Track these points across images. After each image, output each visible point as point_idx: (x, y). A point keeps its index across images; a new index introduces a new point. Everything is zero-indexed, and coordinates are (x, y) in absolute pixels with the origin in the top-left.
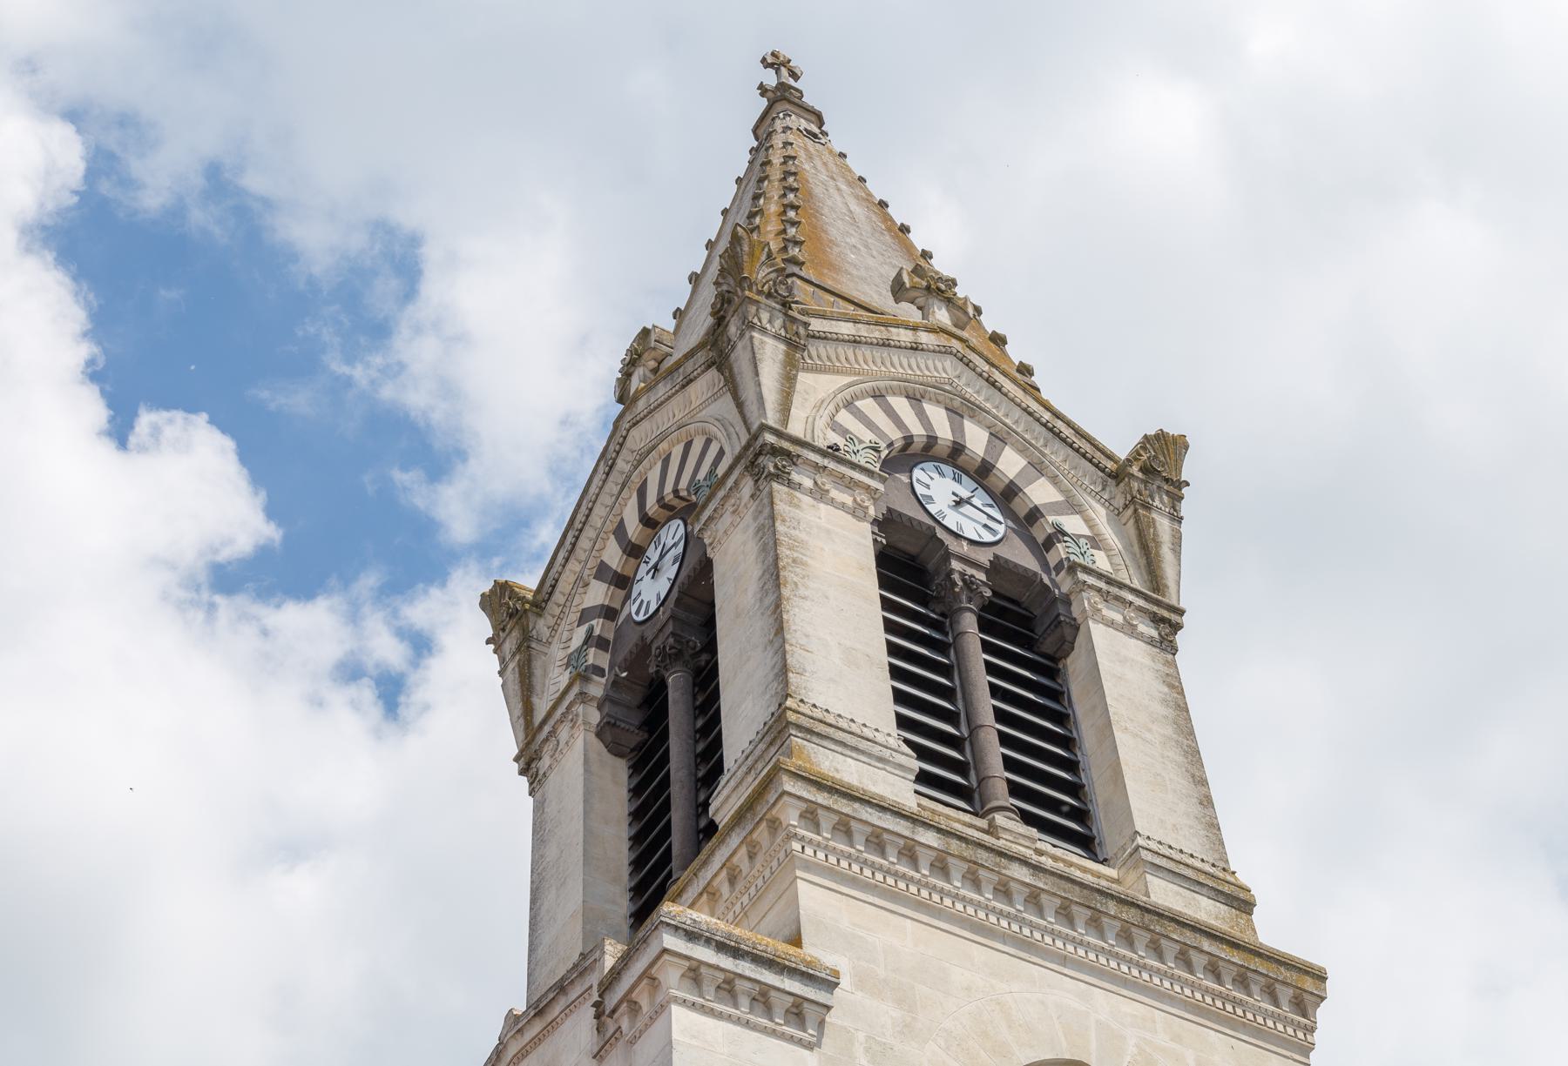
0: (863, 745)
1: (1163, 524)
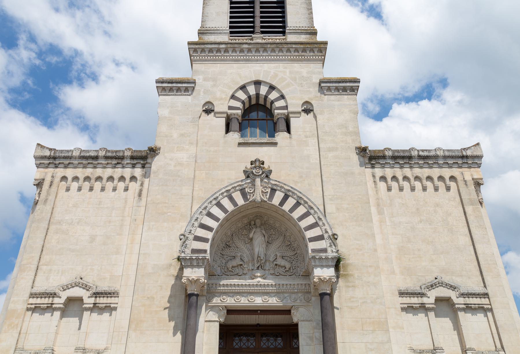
0: (216, 31)
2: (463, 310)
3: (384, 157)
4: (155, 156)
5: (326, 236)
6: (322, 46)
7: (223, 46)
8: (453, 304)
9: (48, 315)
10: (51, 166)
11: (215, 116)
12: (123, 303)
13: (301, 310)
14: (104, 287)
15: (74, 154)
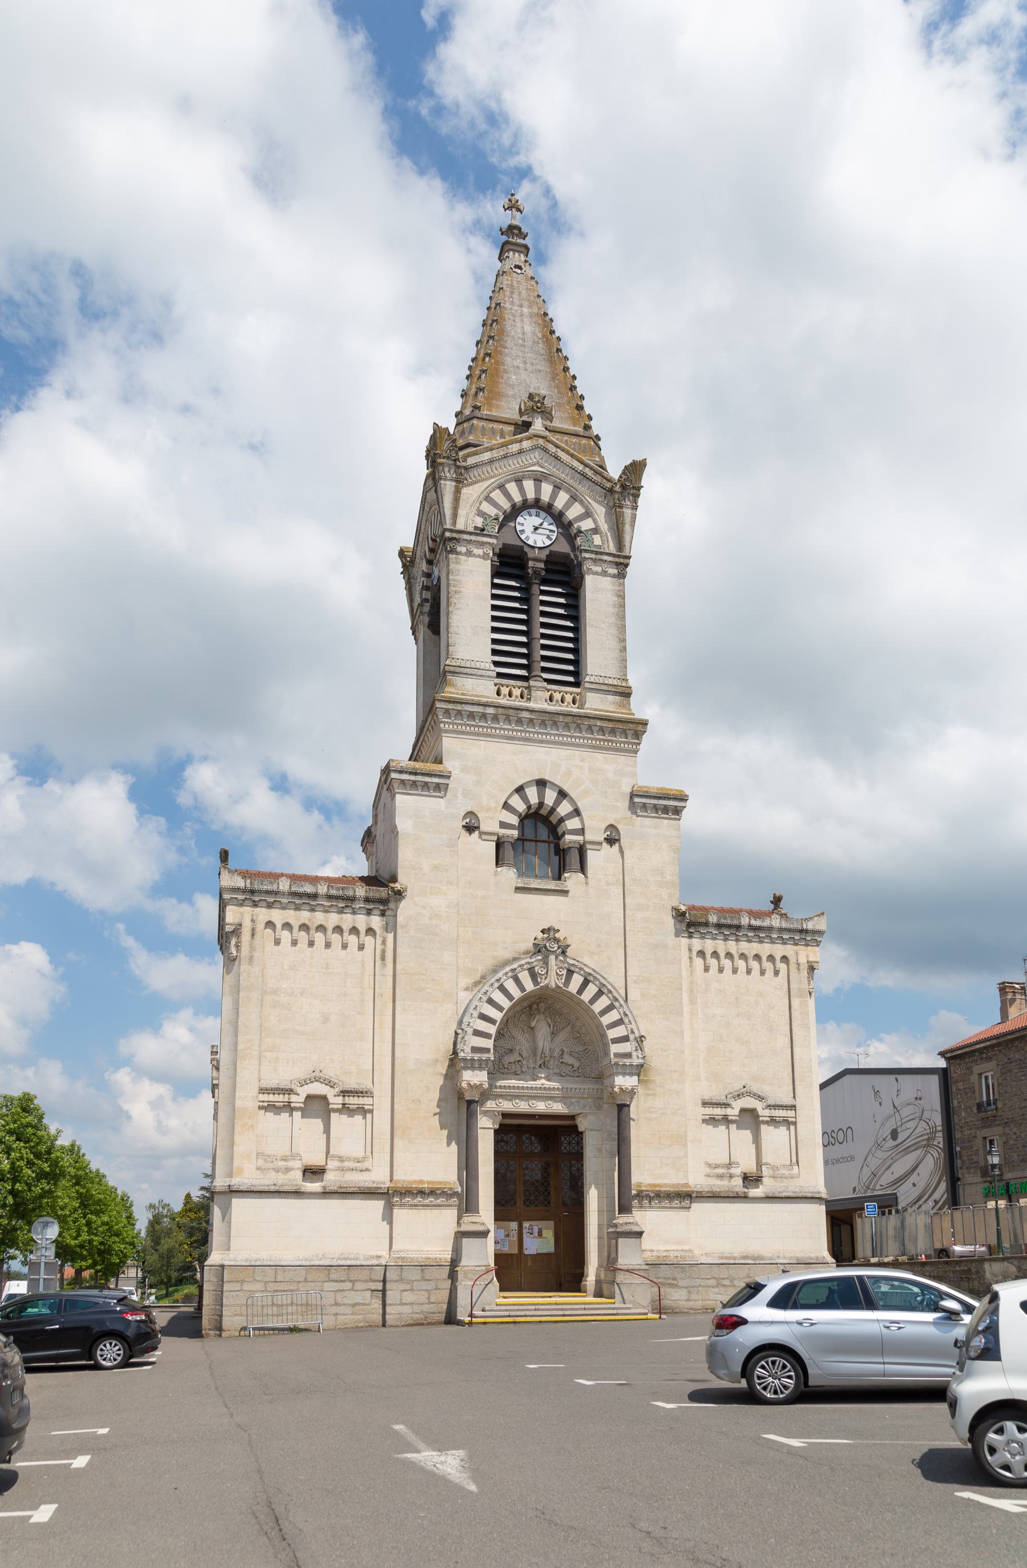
0: (475, 672)
1: (628, 512)
2: (767, 1123)
3: (706, 924)
4: (400, 900)
5: (632, 1037)
6: (640, 728)
7: (490, 711)
8: (758, 1116)
9: (285, 1116)
10: (247, 902)
11: (480, 837)
12: (381, 1103)
13: (590, 1118)
14: (352, 1084)
15: (281, 888)
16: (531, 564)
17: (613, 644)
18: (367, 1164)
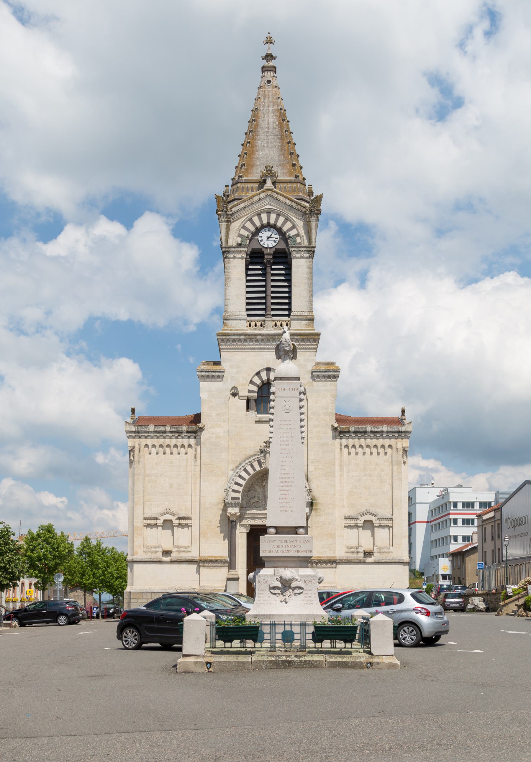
1: (313, 224)
2: (378, 527)
3: (349, 432)
4: (202, 431)
6: (316, 337)
7: (243, 337)
9: (155, 529)
11: (239, 398)
12: (195, 522)
14: (183, 515)
16: (266, 257)
17: (306, 294)
18: (189, 549)
